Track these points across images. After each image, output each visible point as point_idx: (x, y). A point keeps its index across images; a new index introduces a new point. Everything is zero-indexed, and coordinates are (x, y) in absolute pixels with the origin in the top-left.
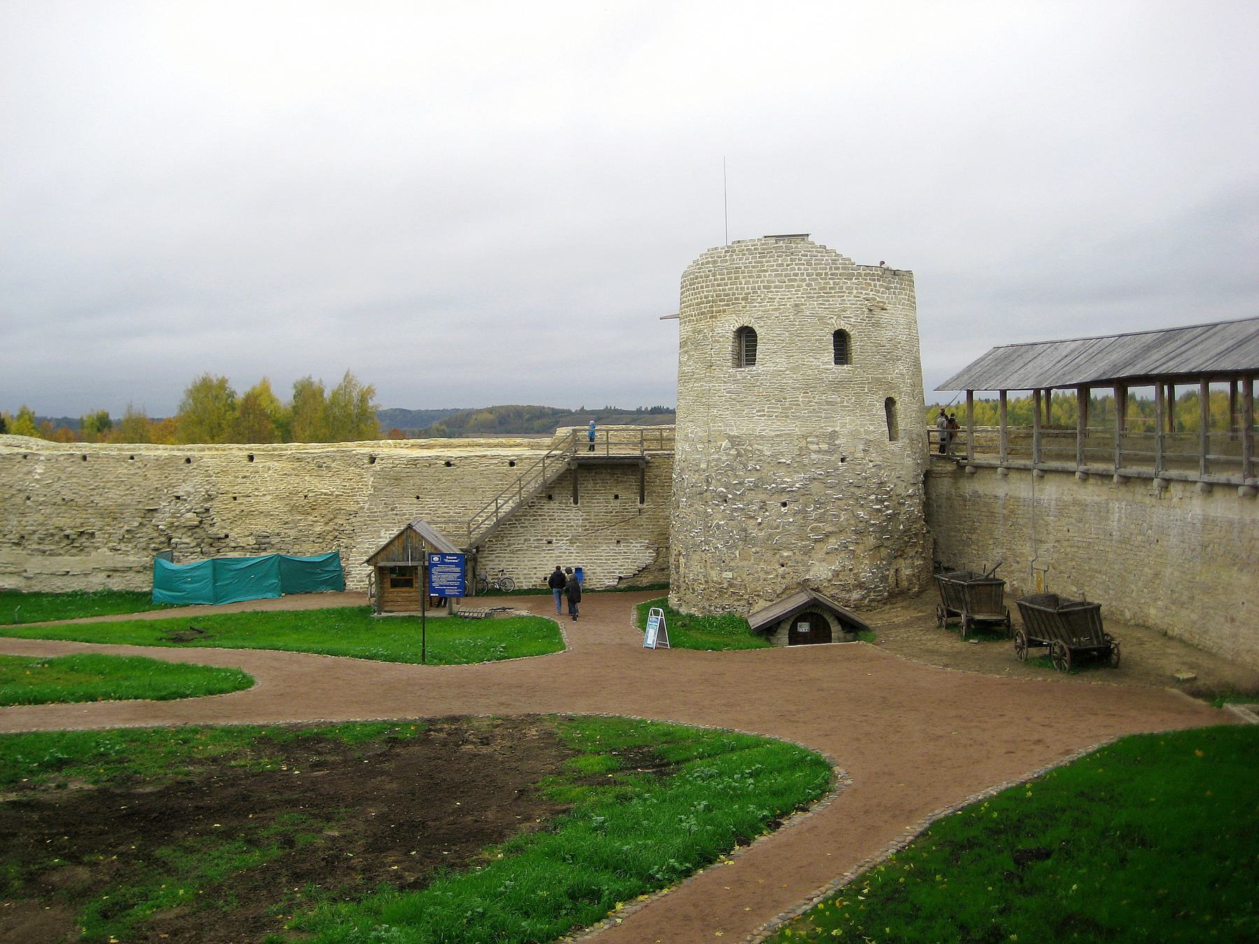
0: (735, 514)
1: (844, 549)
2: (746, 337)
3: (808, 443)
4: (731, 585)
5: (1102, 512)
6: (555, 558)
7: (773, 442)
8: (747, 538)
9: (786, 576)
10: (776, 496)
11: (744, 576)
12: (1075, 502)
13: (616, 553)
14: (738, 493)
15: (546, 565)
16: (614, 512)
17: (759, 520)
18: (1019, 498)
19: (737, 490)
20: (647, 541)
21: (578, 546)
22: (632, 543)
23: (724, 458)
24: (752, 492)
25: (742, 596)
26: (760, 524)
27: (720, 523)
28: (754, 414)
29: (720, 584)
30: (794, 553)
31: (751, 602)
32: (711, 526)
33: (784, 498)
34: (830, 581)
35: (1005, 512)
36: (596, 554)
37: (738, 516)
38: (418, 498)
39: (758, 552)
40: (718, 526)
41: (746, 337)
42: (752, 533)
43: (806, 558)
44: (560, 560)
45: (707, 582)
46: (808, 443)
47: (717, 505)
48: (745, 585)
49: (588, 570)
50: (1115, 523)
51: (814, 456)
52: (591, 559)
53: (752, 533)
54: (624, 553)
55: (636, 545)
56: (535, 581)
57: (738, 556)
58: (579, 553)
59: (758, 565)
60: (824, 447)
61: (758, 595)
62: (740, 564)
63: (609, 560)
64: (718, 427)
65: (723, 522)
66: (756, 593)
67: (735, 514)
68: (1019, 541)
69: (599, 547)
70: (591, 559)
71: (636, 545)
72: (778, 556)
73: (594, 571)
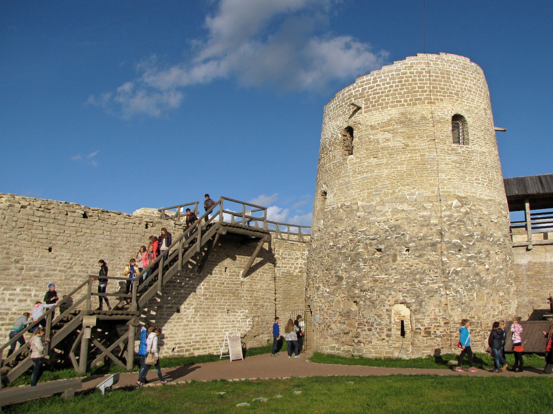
0: (469, 261)
6: (182, 327)
8: (481, 283)
11: (480, 314)
13: (227, 322)
14: (471, 244)
15: (176, 334)
16: (225, 283)
17: (487, 266)
18: (546, 263)
19: (470, 241)
20: (247, 311)
21: (201, 315)
22: (237, 312)
23: (456, 215)
24: (480, 243)
25: (479, 332)
26: (488, 269)
27: (457, 269)
28: (473, 181)
32: (449, 273)
35: (529, 273)
36: (214, 322)
37: (473, 263)
38: (50, 250)
40: (456, 273)
42: (483, 277)
44: (187, 329)
47: (453, 254)
48: (481, 323)
49: (209, 338)
52: (210, 328)
53: (483, 277)
54: (233, 321)
55: (240, 314)
56: (166, 352)
57: (475, 298)
58: (201, 322)
63: (223, 328)
64: (447, 188)
65: (459, 269)
67: (469, 261)
68: (548, 289)
69: (215, 316)
70: (210, 328)
71: (240, 314)
73: (213, 339)
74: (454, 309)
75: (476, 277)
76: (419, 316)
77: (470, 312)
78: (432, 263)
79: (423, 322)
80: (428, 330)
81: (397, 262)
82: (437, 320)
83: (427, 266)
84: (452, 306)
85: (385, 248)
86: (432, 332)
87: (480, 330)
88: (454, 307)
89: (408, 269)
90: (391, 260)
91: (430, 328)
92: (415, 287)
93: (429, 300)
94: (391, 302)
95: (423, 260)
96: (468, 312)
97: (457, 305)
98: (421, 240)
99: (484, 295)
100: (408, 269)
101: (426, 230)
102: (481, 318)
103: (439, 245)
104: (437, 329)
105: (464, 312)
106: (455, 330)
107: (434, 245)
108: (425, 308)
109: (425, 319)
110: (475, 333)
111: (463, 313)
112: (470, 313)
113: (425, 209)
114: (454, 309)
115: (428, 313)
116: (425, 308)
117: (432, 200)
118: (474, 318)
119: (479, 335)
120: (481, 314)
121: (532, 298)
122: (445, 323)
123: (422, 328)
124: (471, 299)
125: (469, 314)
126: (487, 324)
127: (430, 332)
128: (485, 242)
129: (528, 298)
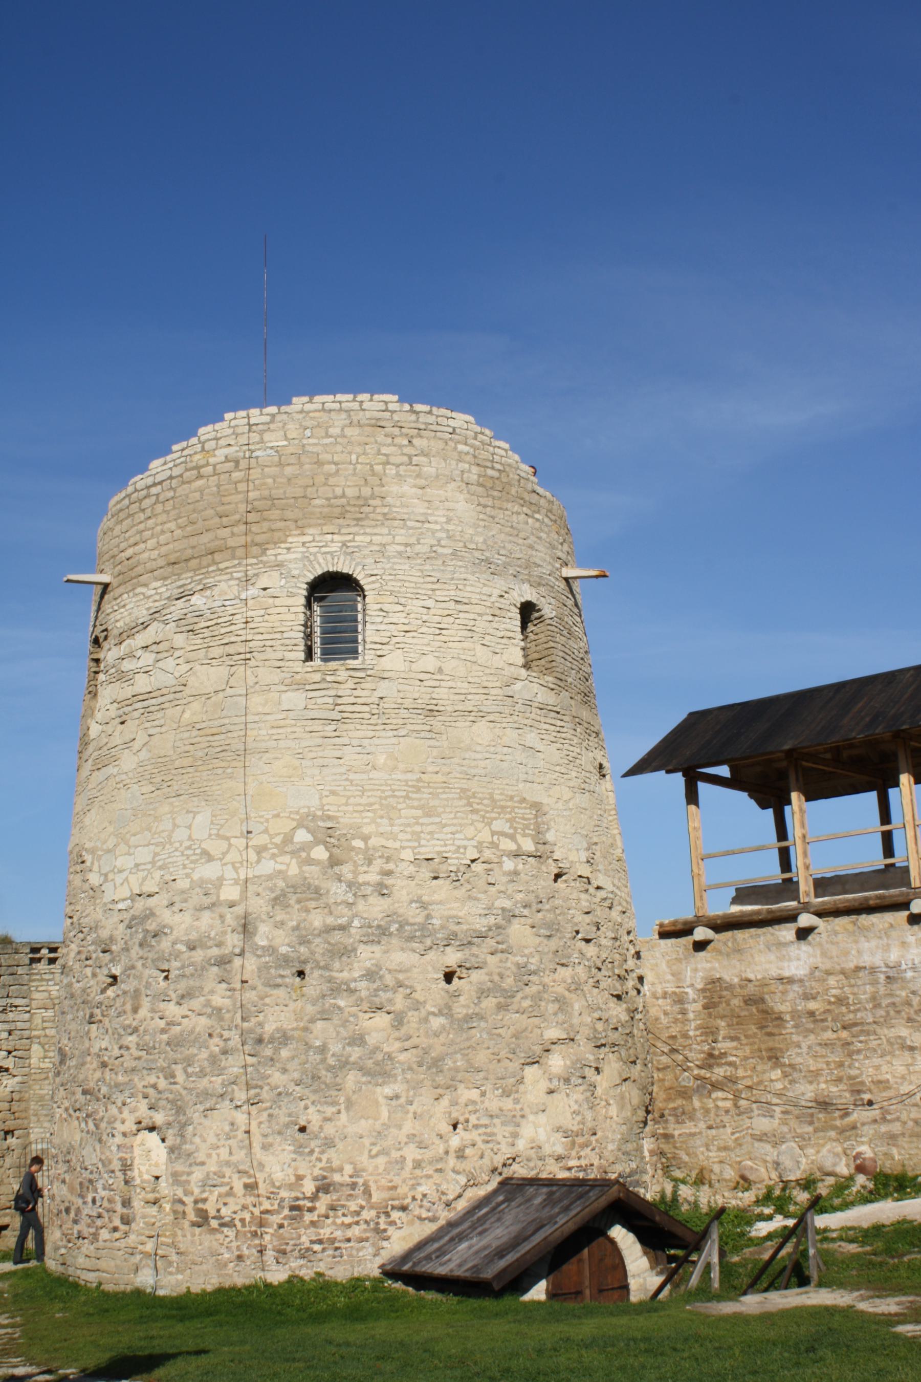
1: (580, 1081)
3: (493, 833)
4: (324, 1187)
7: (418, 828)
9: (468, 1151)
10: (432, 955)
24: (376, 948)
25: (358, 1213)
29: (291, 1187)
30: (483, 1094)
31: (382, 1226)
33: (452, 958)
34: (559, 1158)
39: (397, 1097)
40: (284, 1038)
43: (508, 1104)
45: (250, 1187)
46: (493, 833)
48: (366, 1184)
51: (509, 865)
59: (400, 1127)
60: (528, 845)
61: (404, 1208)
62: (351, 1130)
66: (396, 1203)
68: (867, 1057)
72: (445, 1102)
74: (271, 1145)
75: (348, 1049)
76: (179, 1167)
77: (322, 1152)
78: (217, 1012)
79: (188, 1182)
80: (200, 1205)
81: (143, 1012)
82: (224, 1177)
83: (203, 1022)
84: (265, 1136)
85: (123, 973)
86: (212, 1212)
87: (362, 1207)
88: (270, 1139)
89: (163, 1031)
90: (128, 1007)
91: (205, 1200)
92: (175, 1083)
93: (203, 1120)
94: (127, 1123)
95: (196, 1003)
96: (316, 1155)
97: (280, 1133)
98: (192, 948)
99: (377, 1102)
100: (163, 1031)
101: (210, 921)
102: (363, 1170)
103: (237, 962)
104: (225, 1204)
105: (301, 1154)
106: (276, 1207)
107: (223, 962)
108: (192, 1143)
109: (193, 1173)
110: (344, 1215)
111: (299, 1158)
112: (324, 1157)
113: (210, 858)
114: (271, 1145)
115: (201, 1157)
116: (192, 1143)
117: (228, 835)
118: (341, 1170)
119: (357, 1223)
120: (364, 1158)
121: (823, 1086)
122: (246, 1186)
123: (189, 1200)
124: (328, 1115)
125: (320, 1160)
126: (394, 1188)
127: (206, 1211)
128: (394, 941)
129: (812, 1088)
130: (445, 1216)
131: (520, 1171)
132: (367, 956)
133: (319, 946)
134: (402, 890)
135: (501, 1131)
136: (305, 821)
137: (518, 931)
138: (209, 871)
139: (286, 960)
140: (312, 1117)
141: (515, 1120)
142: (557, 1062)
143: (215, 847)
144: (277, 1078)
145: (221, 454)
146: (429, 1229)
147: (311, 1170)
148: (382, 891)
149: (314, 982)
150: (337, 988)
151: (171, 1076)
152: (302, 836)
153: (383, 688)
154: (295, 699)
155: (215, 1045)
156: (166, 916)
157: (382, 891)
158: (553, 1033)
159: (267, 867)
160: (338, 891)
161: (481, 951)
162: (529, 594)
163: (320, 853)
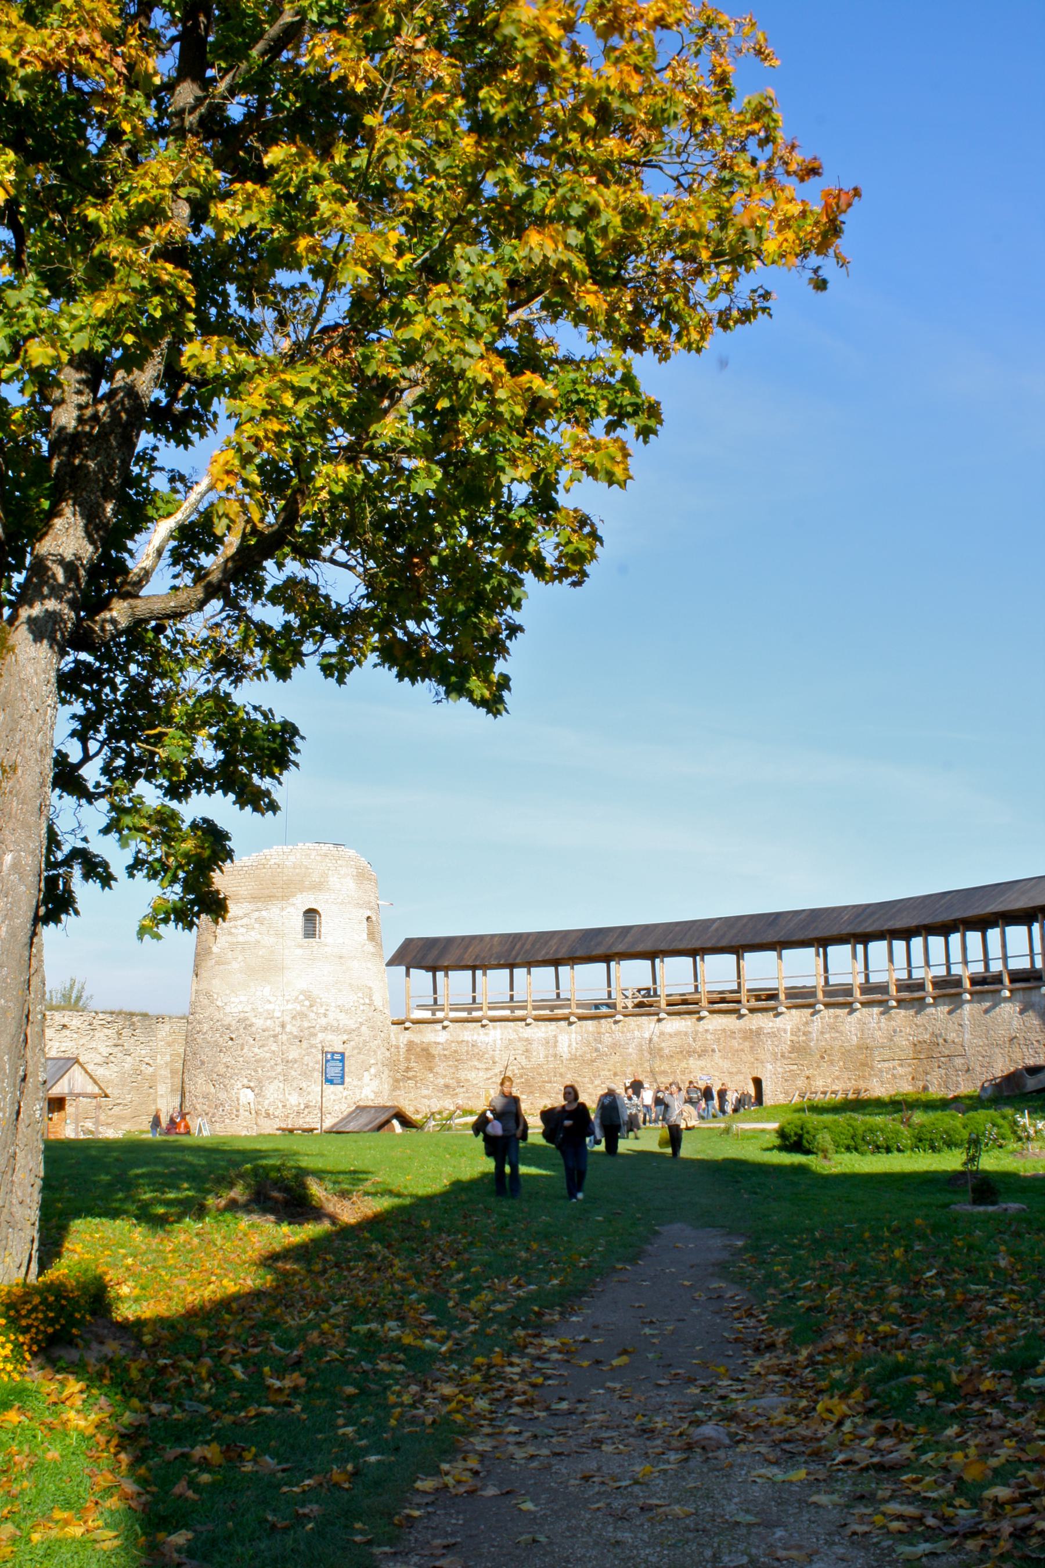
2: (311, 914)
4: (307, 1107)
5: (551, 1043)
12: (520, 1039)
33: (345, 1037)
40: (296, 1061)
41: (311, 914)
50: (566, 1049)
107: (275, 1036)
130: (341, 1116)
131: (362, 1104)
132: (321, 1036)
133: (306, 1032)
134: (331, 1016)
135: (357, 1091)
136: (302, 992)
137: (364, 1028)
138: (270, 1007)
139: (296, 1037)
140: (304, 1085)
141: (361, 1088)
142: (373, 1071)
143: (272, 999)
144: (293, 1073)
145: (272, 862)
146: (337, 1120)
147: (303, 1102)
148: (325, 1015)
149: (305, 1044)
150: (312, 1046)
151: (256, 1071)
152: (301, 997)
153: (326, 949)
154: (299, 951)
155: (272, 1062)
156: (254, 1020)
157: (325, 1015)
158: (372, 1061)
159: (290, 1006)
160: (312, 1015)
161: (354, 1035)
162: (369, 913)
163: (307, 1003)
